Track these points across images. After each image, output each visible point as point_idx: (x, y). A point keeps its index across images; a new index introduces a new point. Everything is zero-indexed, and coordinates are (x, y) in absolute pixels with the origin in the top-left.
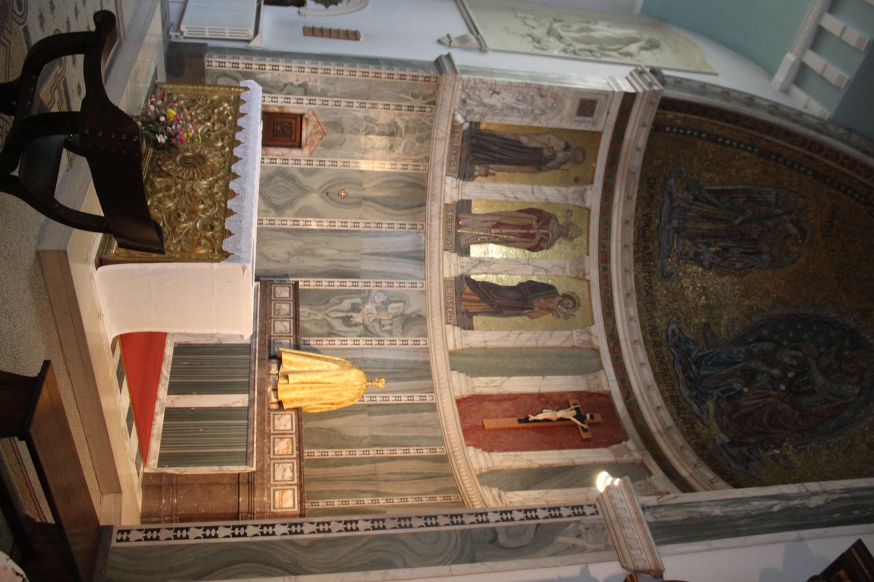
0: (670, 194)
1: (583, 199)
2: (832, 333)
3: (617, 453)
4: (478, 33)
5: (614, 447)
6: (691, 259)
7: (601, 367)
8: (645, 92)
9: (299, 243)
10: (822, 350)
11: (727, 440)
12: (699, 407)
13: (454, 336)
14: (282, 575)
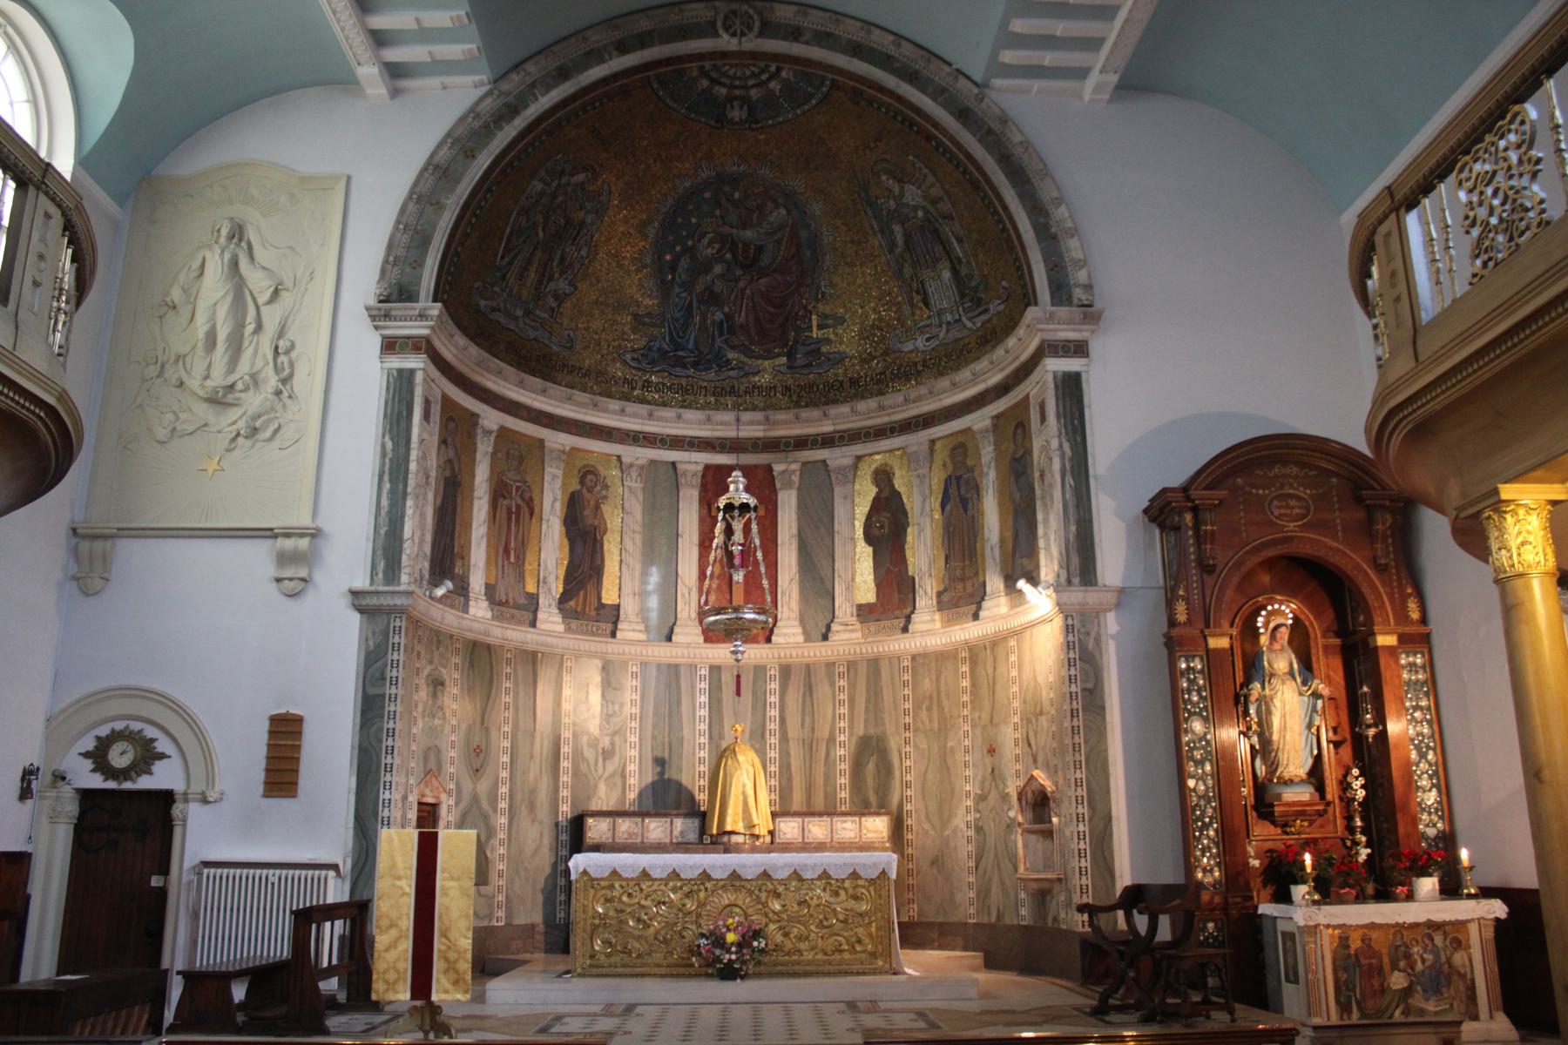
0: (494, 310)
1: (490, 432)
2: (707, 195)
3: (788, 485)
4: (272, 529)
5: (778, 485)
6: (559, 306)
7: (674, 464)
8: (432, 328)
9: (523, 808)
10: (718, 212)
11: (784, 360)
12: (732, 369)
13: (629, 630)
14: (1111, 828)
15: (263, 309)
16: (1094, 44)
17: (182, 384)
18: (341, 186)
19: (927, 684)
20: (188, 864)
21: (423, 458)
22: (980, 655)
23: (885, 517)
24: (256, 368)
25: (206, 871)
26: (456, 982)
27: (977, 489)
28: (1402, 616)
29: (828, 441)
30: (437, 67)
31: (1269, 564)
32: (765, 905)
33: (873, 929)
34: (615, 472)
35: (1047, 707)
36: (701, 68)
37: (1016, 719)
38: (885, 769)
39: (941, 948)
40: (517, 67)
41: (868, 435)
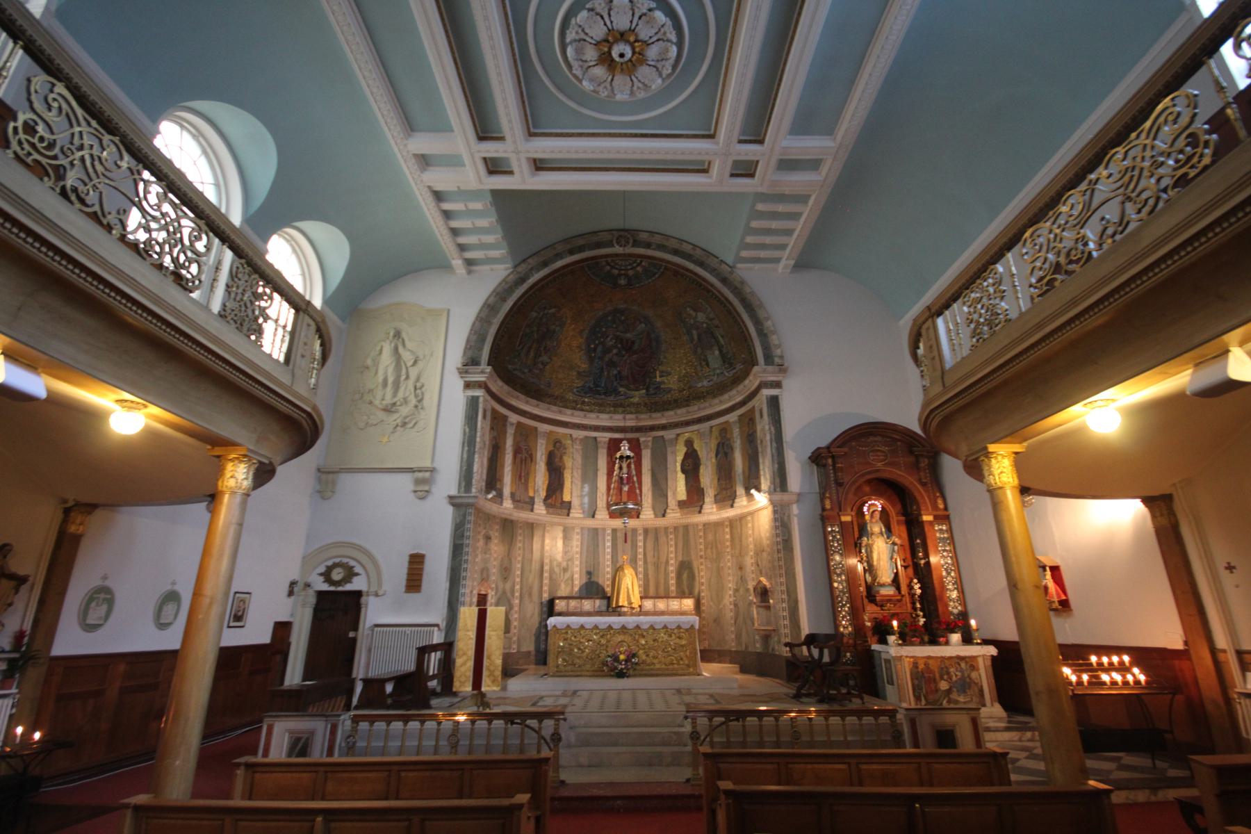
0: (514, 370)
2: (610, 318)
3: (647, 447)
5: (642, 447)
7: (595, 438)
8: (487, 377)
11: (644, 391)
15: (410, 369)
16: (783, 247)
17: (371, 403)
18: (445, 314)
19: (710, 537)
21: (483, 435)
22: (736, 524)
23: (690, 461)
24: (406, 395)
25: (376, 629)
26: (493, 682)
27: (732, 449)
28: (935, 507)
29: (664, 427)
30: (489, 261)
31: (869, 482)
32: (638, 641)
33: (688, 653)
34: (569, 442)
35: (766, 548)
36: (607, 262)
37: (752, 553)
38: (692, 577)
39: (720, 662)
40: (524, 261)
41: (682, 424)
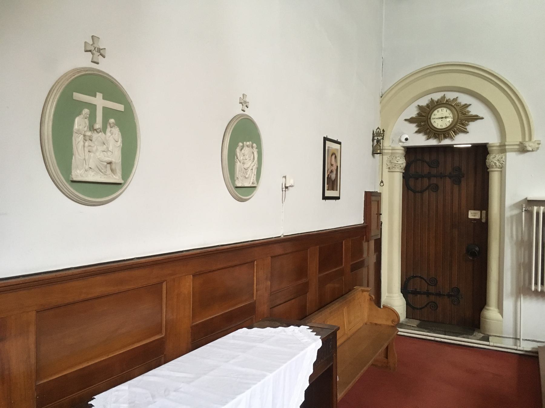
20: (509, 201)
